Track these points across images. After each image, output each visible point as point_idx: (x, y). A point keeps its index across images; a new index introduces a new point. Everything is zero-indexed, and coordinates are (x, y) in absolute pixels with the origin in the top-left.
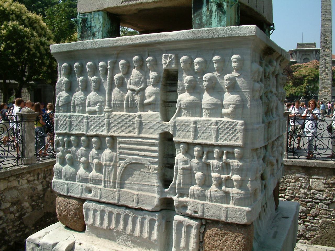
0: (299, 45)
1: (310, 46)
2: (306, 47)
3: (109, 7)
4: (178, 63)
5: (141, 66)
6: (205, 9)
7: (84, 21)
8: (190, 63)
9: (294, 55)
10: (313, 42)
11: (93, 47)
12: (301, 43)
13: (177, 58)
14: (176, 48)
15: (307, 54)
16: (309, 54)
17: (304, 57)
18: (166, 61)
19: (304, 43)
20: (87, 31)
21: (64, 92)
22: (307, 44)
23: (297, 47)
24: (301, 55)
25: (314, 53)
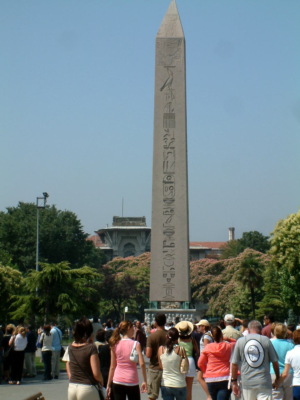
0: (117, 220)
1: (136, 222)
2: (129, 225)
4: (180, 316)
5: (171, 316)
6: (183, 304)
7: (152, 303)
8: (182, 316)
9: (108, 239)
10: (141, 216)
11: (158, 311)
12: (121, 216)
13: (180, 315)
14: (180, 313)
15: (131, 237)
16: (133, 237)
17: (126, 242)
18: (177, 315)
19: (124, 216)
20: (152, 306)
21: (149, 321)
22: (131, 219)
23: (114, 224)
24: (120, 238)
25: (143, 235)
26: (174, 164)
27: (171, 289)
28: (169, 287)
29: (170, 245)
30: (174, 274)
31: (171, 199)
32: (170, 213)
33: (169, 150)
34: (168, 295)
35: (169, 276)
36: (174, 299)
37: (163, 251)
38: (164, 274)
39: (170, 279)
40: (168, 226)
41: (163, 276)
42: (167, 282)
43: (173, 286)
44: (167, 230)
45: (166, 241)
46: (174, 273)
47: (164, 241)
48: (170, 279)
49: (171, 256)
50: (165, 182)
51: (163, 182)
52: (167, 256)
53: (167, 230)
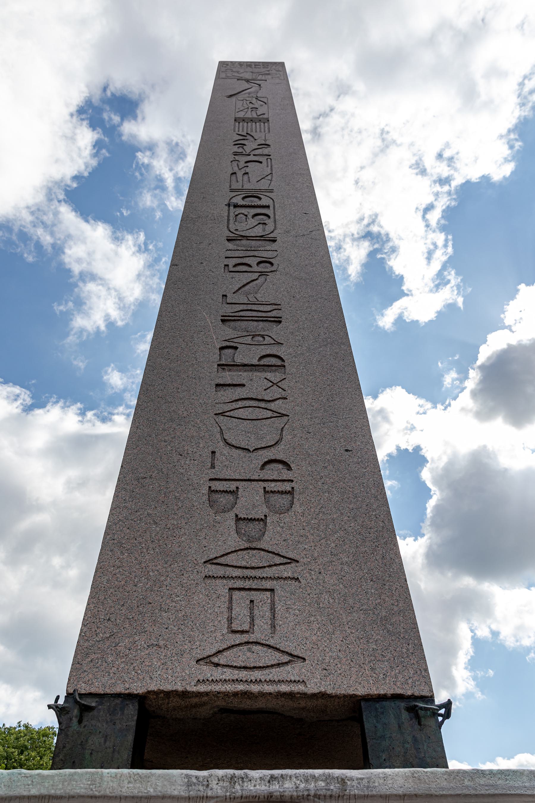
3: (161, 688)
26: (269, 177)
27: (272, 590)
28: (253, 573)
29: (255, 362)
30: (291, 492)
31: (262, 236)
32: (255, 268)
33: (252, 158)
34: (244, 638)
35: (251, 502)
36: (292, 672)
37: (217, 385)
38: (211, 491)
39: (263, 520)
40: (246, 302)
41: (212, 503)
42: (234, 541)
43: (287, 571)
44: (242, 314)
45: (236, 348)
46: (287, 487)
47: (222, 348)
48: (263, 520)
49: (263, 405)
50: (236, 206)
51: (229, 205)
52: (240, 404)
53: (242, 314)
